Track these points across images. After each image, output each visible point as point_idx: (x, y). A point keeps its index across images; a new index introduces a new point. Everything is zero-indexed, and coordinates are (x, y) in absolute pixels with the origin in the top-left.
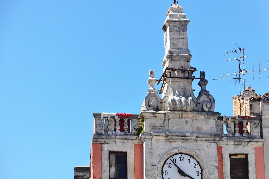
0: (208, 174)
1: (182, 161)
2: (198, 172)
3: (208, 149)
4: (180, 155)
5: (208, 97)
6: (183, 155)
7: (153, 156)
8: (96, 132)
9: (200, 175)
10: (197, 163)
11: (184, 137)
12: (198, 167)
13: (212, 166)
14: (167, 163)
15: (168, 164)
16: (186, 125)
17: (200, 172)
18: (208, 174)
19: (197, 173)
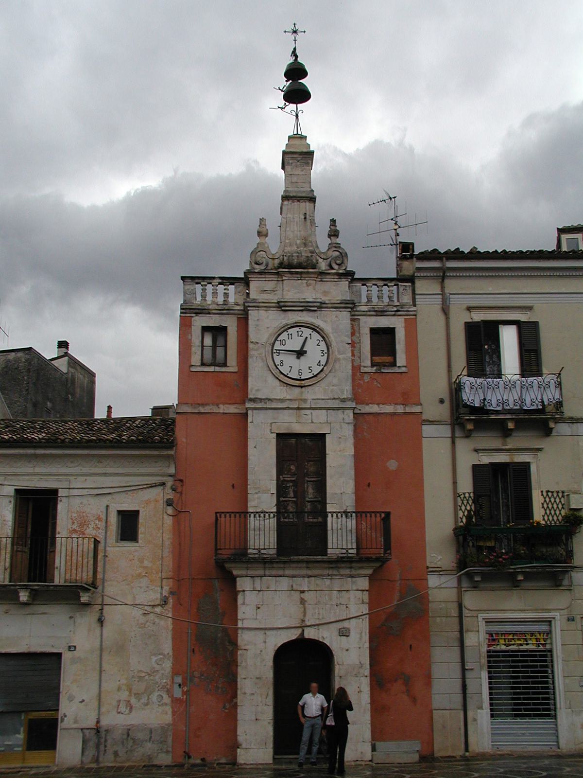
0: (336, 353)
1: (300, 336)
2: (323, 351)
3: (338, 319)
4: (297, 329)
5: (338, 251)
6: (302, 329)
7: (259, 330)
8: (185, 301)
9: (326, 355)
10: (321, 339)
11: (307, 307)
12: (323, 344)
13: (342, 342)
14: (279, 339)
15: (280, 341)
16: (307, 288)
17: (326, 351)
18: (336, 353)
19: (322, 353)
